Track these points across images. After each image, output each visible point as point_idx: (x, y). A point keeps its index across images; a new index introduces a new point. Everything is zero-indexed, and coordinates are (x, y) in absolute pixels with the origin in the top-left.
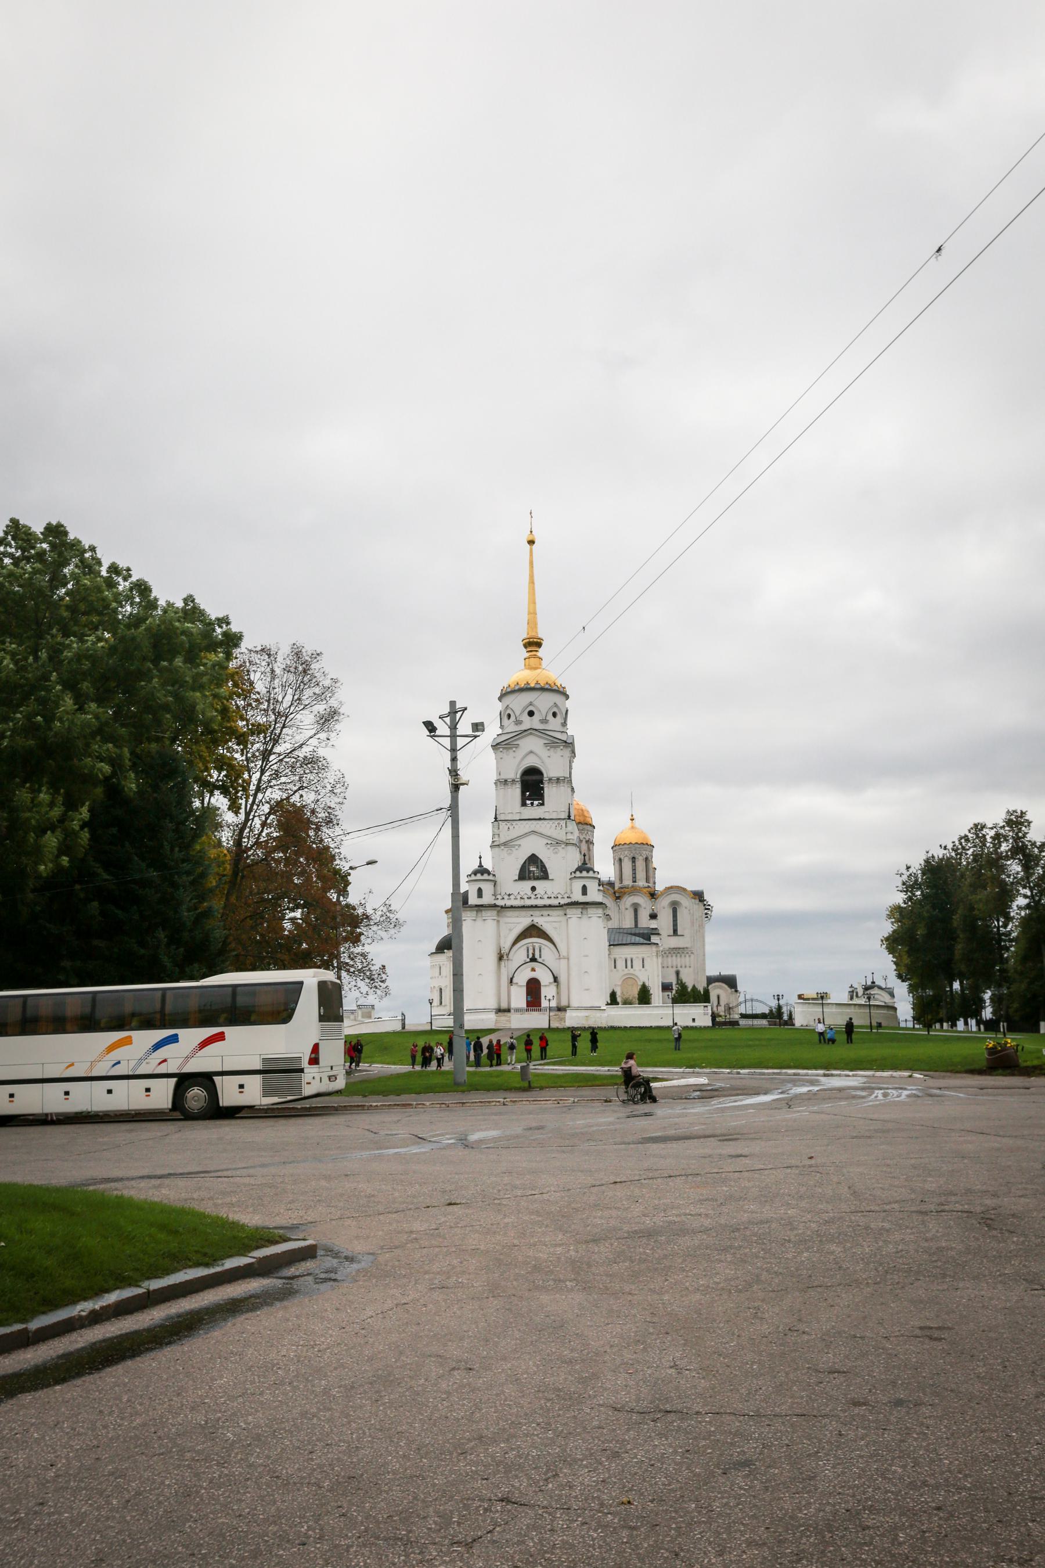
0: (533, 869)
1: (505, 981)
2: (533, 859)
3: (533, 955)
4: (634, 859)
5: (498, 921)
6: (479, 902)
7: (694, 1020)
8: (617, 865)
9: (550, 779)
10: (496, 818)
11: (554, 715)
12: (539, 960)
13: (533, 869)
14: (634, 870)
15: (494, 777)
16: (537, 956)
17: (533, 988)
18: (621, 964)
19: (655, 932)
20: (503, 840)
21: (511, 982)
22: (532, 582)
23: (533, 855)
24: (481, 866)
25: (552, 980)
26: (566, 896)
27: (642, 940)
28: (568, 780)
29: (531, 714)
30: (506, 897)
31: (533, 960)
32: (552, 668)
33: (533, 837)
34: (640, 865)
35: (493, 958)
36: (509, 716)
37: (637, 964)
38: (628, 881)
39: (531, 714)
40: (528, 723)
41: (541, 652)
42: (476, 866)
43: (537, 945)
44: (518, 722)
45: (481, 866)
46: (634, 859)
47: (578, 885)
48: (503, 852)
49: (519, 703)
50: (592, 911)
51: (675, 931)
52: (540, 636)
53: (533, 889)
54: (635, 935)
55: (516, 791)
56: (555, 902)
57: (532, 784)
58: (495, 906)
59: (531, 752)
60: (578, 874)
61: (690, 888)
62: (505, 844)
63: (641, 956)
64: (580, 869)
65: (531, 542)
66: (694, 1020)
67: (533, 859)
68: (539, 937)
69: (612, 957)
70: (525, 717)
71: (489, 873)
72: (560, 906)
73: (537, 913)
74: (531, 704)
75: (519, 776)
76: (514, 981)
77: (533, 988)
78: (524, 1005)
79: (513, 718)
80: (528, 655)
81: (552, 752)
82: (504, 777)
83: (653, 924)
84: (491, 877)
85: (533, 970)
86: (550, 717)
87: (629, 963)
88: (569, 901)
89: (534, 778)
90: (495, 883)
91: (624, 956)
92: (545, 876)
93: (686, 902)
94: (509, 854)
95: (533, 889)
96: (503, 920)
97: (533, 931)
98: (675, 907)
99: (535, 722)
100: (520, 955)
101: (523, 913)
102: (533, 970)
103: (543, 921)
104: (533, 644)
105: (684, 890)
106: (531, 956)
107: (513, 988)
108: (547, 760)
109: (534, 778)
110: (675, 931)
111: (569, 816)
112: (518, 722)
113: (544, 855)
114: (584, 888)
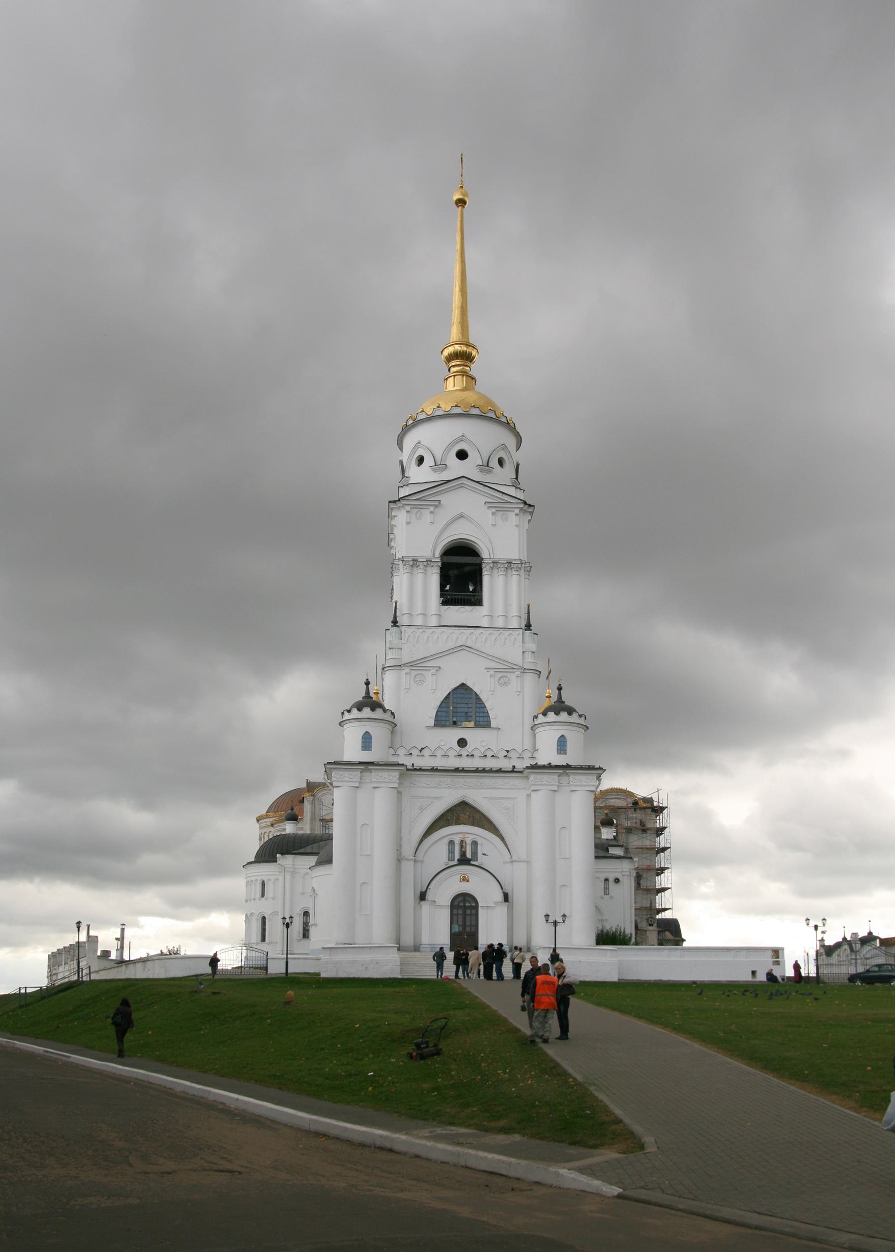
0: (462, 708)
1: (409, 895)
3: (463, 854)
6: (366, 757)
13: (462, 708)
16: (469, 855)
17: (464, 908)
21: (423, 896)
23: (463, 685)
25: (500, 897)
30: (415, 752)
31: (464, 861)
36: (421, 460)
39: (462, 455)
40: (456, 468)
44: (439, 466)
53: (462, 743)
56: (506, 765)
59: (461, 516)
62: (412, 665)
68: (473, 824)
70: (453, 460)
72: (513, 770)
73: (472, 780)
74: (462, 438)
75: (438, 553)
76: (429, 896)
77: (464, 908)
79: (428, 461)
92: (483, 721)
95: (462, 743)
97: (462, 813)
100: (437, 851)
101: (447, 779)
102: (465, 879)
106: (457, 856)
113: (482, 686)
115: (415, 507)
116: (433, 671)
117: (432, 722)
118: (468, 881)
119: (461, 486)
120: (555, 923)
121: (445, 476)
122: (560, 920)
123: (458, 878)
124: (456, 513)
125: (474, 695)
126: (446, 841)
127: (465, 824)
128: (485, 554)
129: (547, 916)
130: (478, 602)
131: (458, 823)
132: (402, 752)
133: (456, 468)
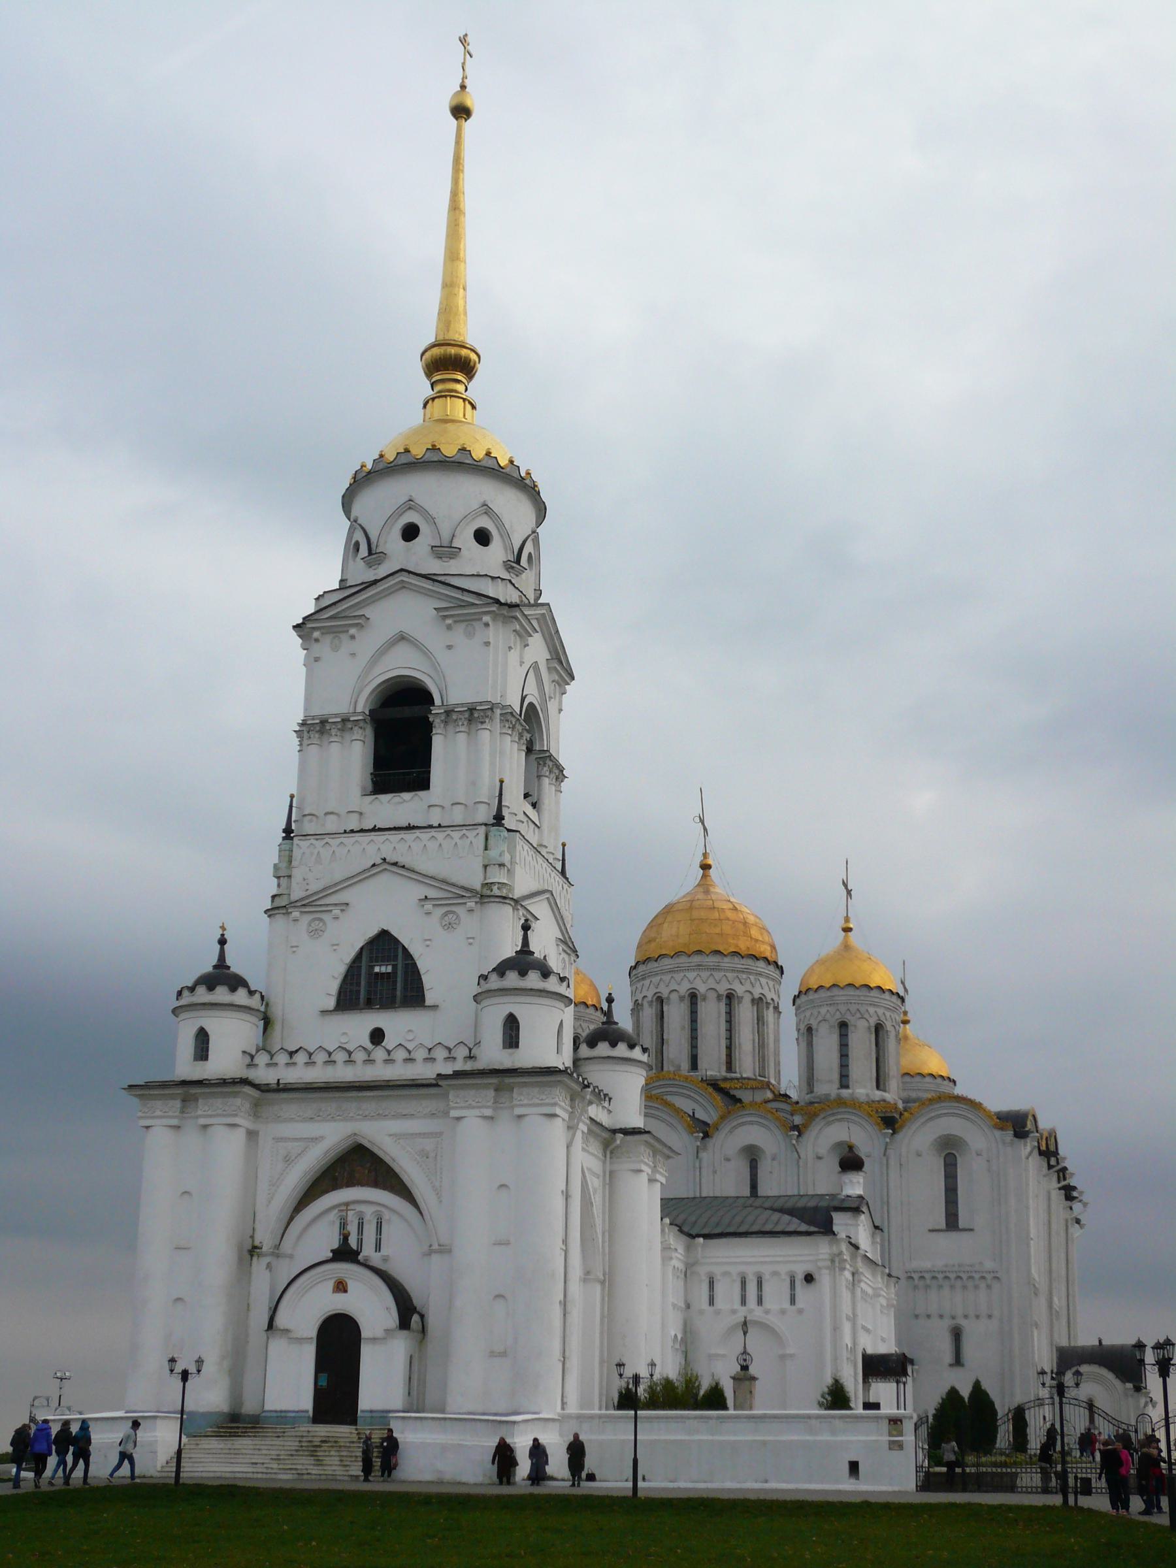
0: (383, 977)
2: (384, 945)
4: (843, 1025)
5: (252, 1135)
7: (854, 1467)
8: (804, 1045)
9: (448, 713)
10: (288, 831)
11: (483, 537)
12: (376, 1259)
13: (383, 977)
14: (844, 1055)
15: (300, 718)
17: (339, 1343)
18: (727, 1293)
19: (854, 1207)
20: (297, 893)
22: (455, 207)
24: (221, 964)
25: (393, 1319)
26: (462, 1052)
27: (804, 1227)
28: (530, 722)
29: (410, 532)
30: (282, 1058)
31: (345, 1253)
32: (493, 419)
33: (387, 881)
34: (861, 1043)
35: (218, 1251)
37: (775, 1294)
38: (827, 1087)
39: (410, 532)
40: (398, 553)
41: (476, 388)
42: (207, 965)
43: (369, 1212)
45: (221, 964)
46: (843, 1025)
47: (494, 1015)
48: (299, 927)
49: (379, 503)
50: (525, 1098)
51: (952, 1222)
52: (470, 341)
53: (377, 1036)
54: (791, 1212)
55: (354, 755)
56: (428, 1072)
57: (401, 735)
58: (245, 1082)
59: (402, 638)
60: (495, 982)
61: (997, 1103)
63: (784, 1269)
64: (502, 969)
65: (461, 112)
66: (854, 1467)
67: (384, 945)
68: (376, 1184)
69: (703, 1270)
70: (393, 543)
71: (236, 982)
74: (410, 505)
75: (363, 705)
77: (339, 1343)
78: (306, 1402)
80: (429, 393)
81: (458, 635)
82: (317, 711)
83: (854, 1185)
84: (241, 997)
85: (341, 1287)
86: (466, 540)
87: (752, 1287)
88: (468, 1066)
89: (407, 712)
90: (267, 1022)
91: (735, 1270)
93: (979, 1140)
94: (315, 933)
95: (377, 1036)
96: (270, 1131)
98: (950, 1153)
99: (418, 556)
101: (329, 1105)
102: (341, 1287)
103: (388, 1132)
104: (450, 364)
105: (974, 1105)
107: (277, 1346)
108: (441, 656)
109: (407, 712)
110: (952, 1222)
111: (499, 818)
112: (374, 555)
114: (512, 1025)
115: (326, 631)
116: (336, 911)
117: (331, 1003)
118: (345, 1291)
119: (403, 586)
120: (185, 1376)
121: (382, 571)
122: (192, 1369)
123: (331, 1285)
124: (390, 632)
125: (400, 950)
126: (333, 1216)
127: (362, 1185)
128: (437, 702)
129: (172, 1360)
130: (423, 783)
131: (351, 1183)
132: (262, 1059)
133: (398, 553)
